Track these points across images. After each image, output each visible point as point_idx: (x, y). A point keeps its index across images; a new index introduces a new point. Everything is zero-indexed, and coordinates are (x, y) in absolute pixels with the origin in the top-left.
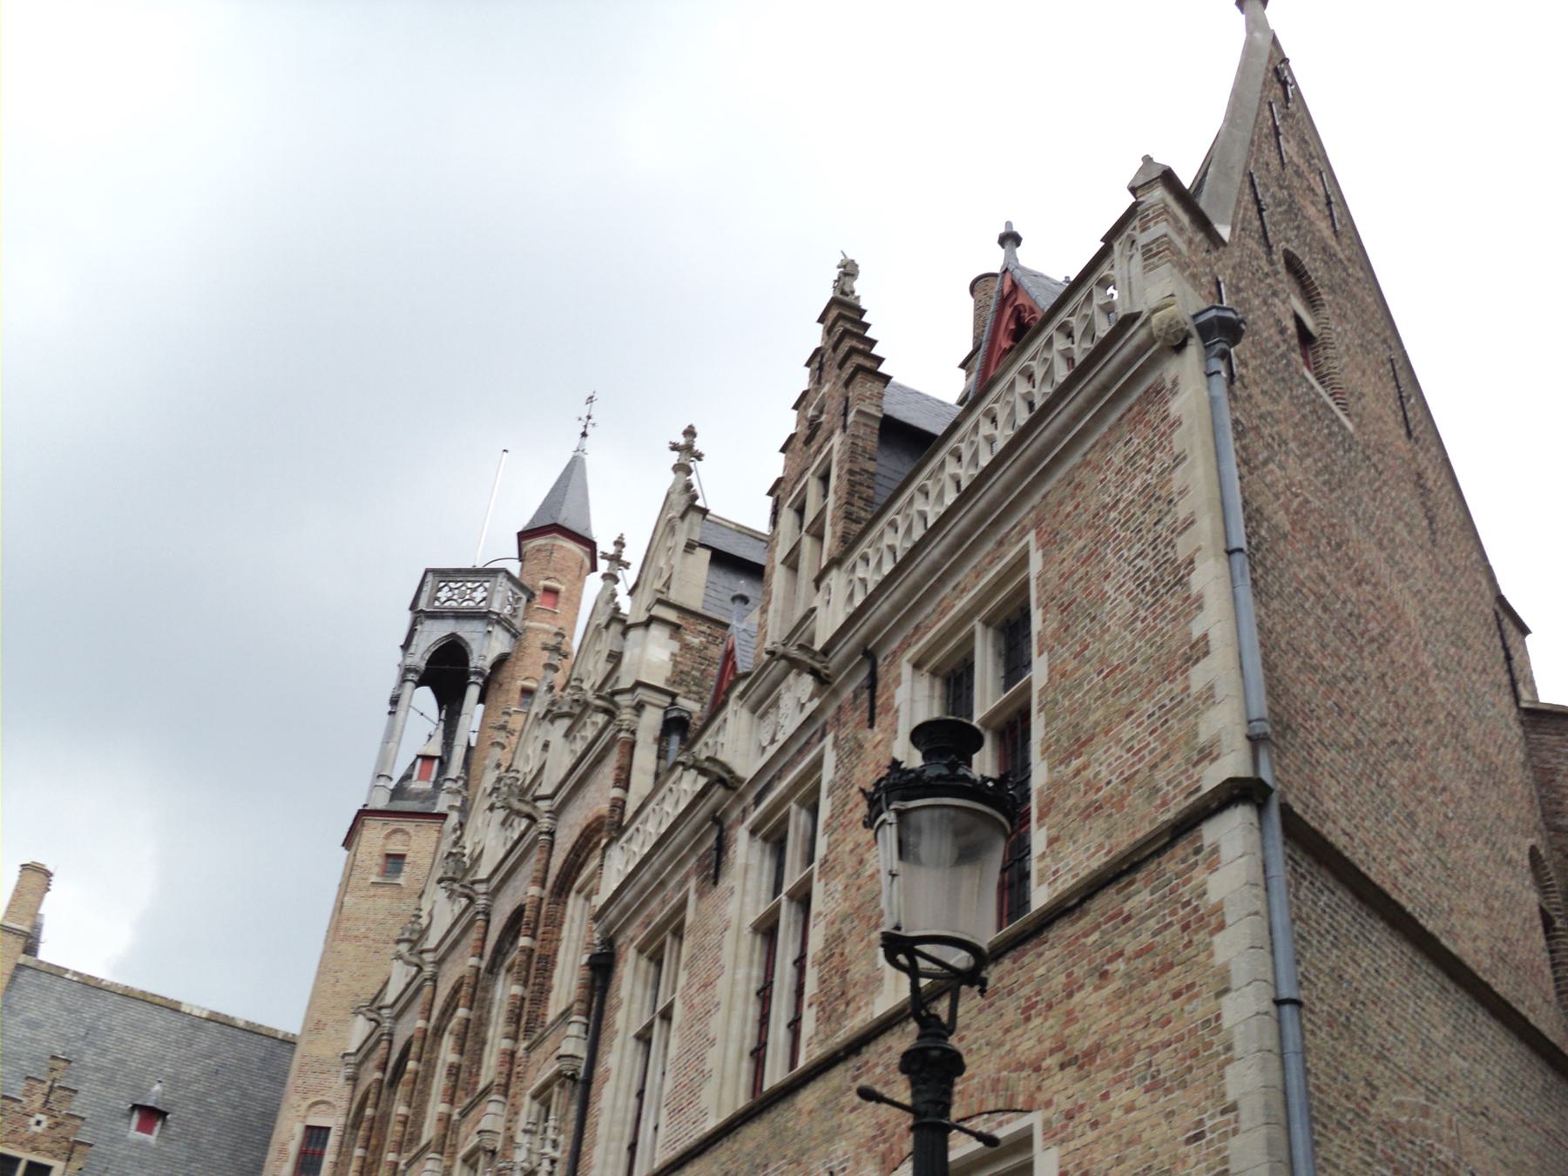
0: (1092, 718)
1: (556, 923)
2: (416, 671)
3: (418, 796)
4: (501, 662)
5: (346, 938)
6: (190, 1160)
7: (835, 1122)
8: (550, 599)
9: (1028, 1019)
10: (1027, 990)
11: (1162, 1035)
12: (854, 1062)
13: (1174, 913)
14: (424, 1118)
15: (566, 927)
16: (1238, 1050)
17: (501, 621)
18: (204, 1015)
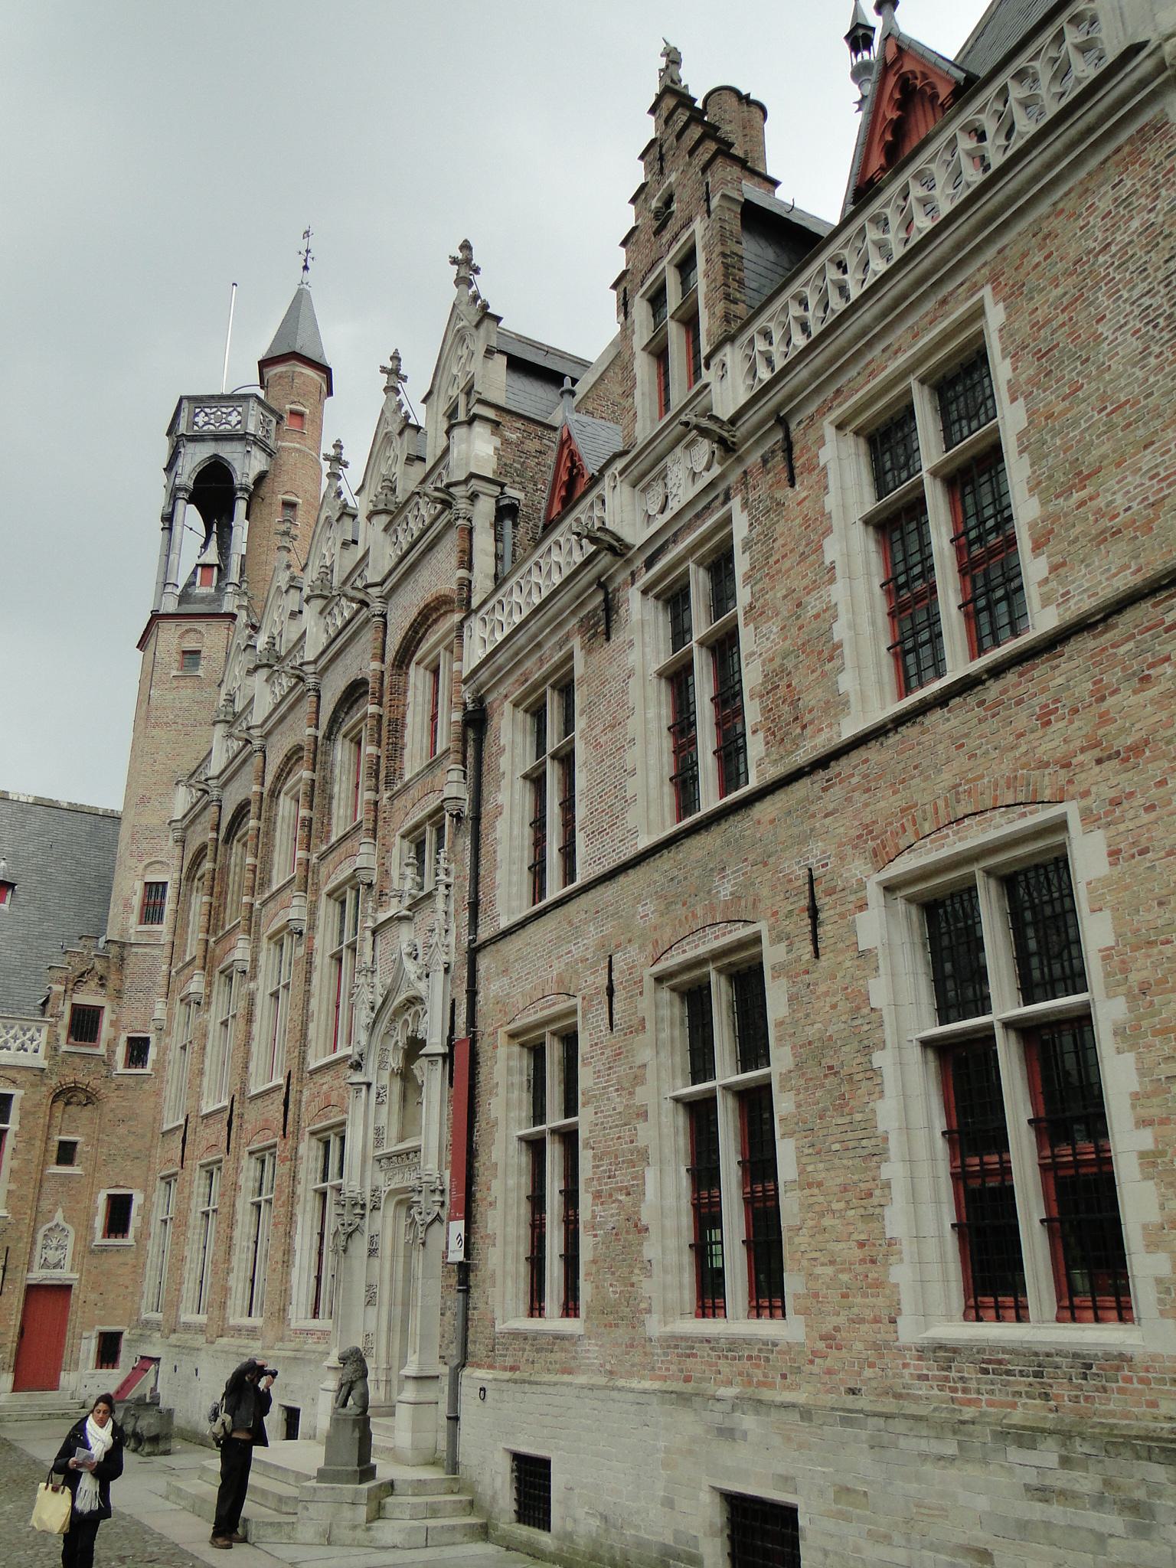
0: (1096, 453)
1: (399, 691)
2: (186, 490)
3: (203, 599)
4: (261, 478)
5: (156, 725)
6: (41, 921)
7: (806, 827)
8: (296, 420)
9: (1049, 723)
10: (1042, 699)
12: (821, 775)
14: (272, 865)
15: (410, 693)
17: (257, 442)
18: (31, 800)
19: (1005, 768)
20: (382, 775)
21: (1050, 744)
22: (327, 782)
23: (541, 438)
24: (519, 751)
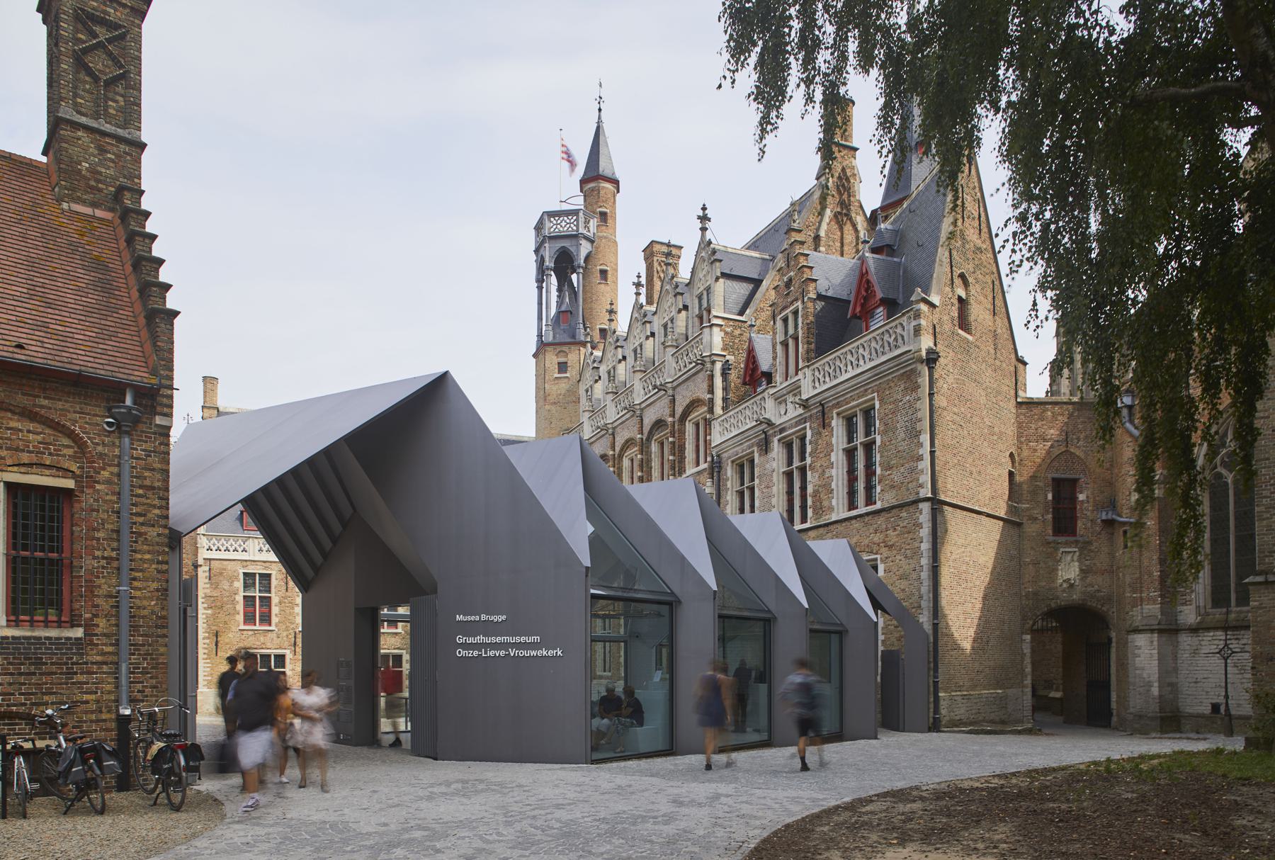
1: (682, 432)
15: (687, 434)
19: (866, 542)
20: (677, 469)
21: (876, 539)
22: (649, 461)
24: (734, 480)
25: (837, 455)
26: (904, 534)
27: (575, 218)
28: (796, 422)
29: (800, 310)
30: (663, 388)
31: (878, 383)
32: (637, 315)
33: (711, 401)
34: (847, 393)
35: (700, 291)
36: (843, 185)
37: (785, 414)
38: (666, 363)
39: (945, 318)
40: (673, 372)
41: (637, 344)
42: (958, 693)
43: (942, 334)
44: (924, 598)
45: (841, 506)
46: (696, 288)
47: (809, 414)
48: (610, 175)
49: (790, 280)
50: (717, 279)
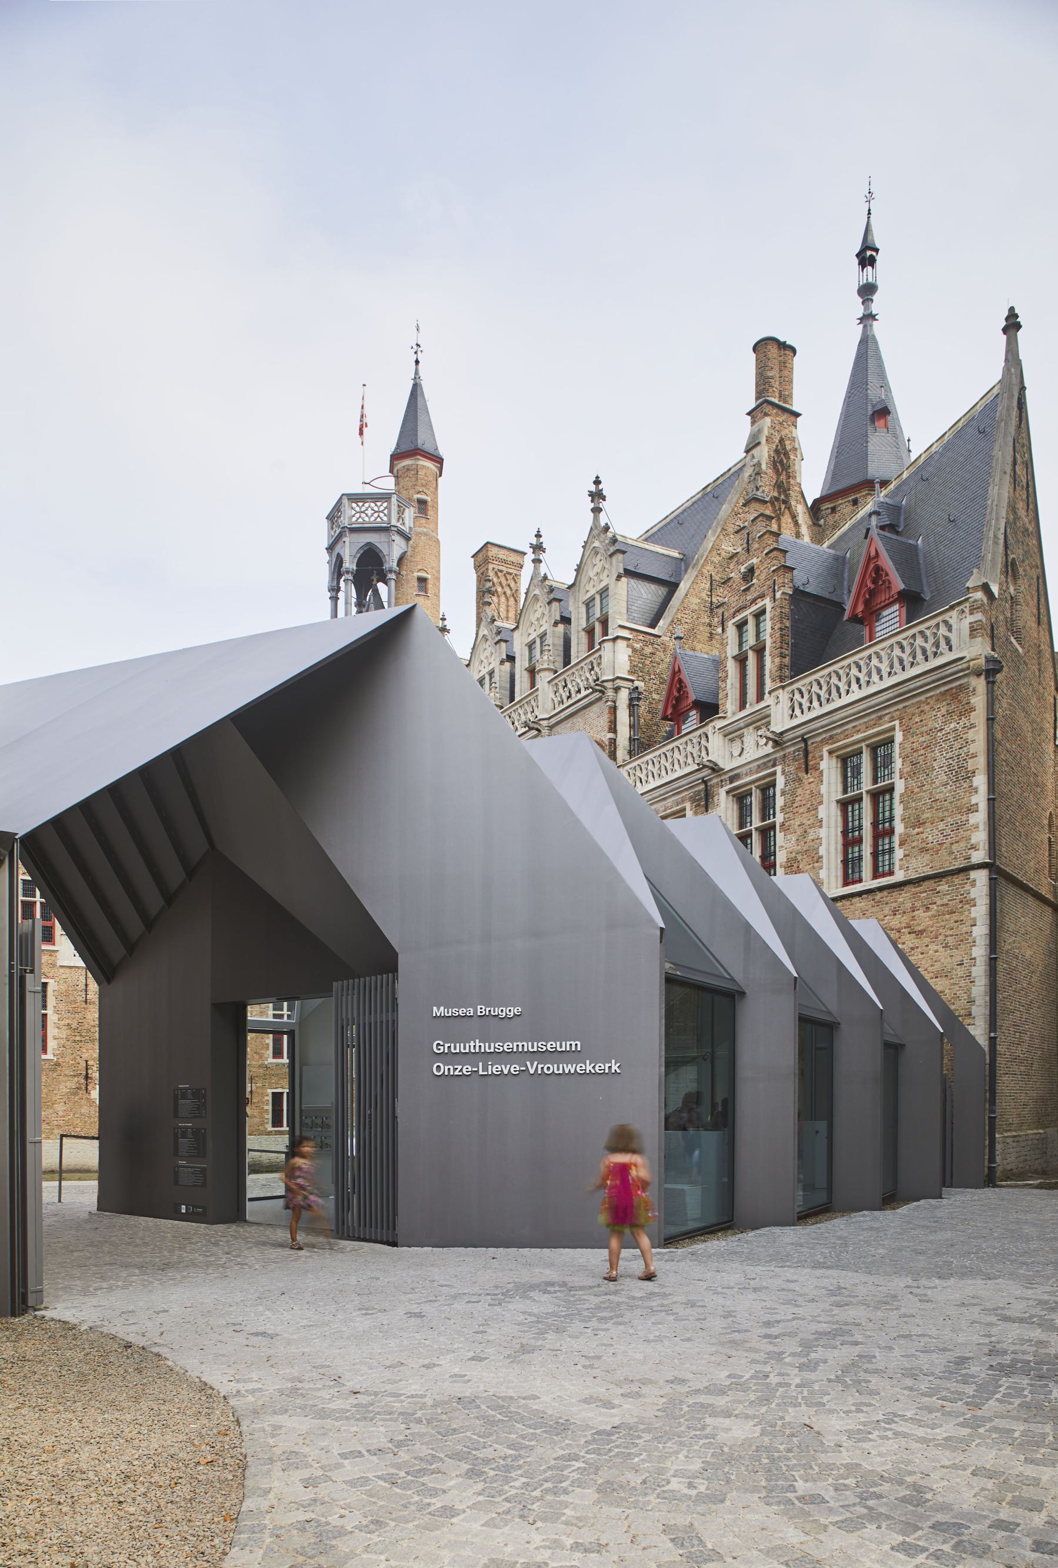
11: (951, 933)
13: (957, 896)
16: (977, 943)
23: (652, 644)
25: (828, 808)
26: (944, 915)
27: (385, 504)
28: (759, 766)
29: (768, 610)
30: (536, 726)
31: (900, 706)
32: (486, 632)
33: (613, 742)
34: (847, 723)
35: (589, 595)
36: (781, 462)
37: (740, 755)
38: (539, 693)
39: (1001, 617)
40: (550, 705)
41: (484, 672)
42: (1009, 1134)
43: (999, 638)
44: (977, 1003)
45: (833, 879)
46: (582, 591)
47: (782, 753)
48: (431, 451)
49: (751, 570)
50: (619, 577)
